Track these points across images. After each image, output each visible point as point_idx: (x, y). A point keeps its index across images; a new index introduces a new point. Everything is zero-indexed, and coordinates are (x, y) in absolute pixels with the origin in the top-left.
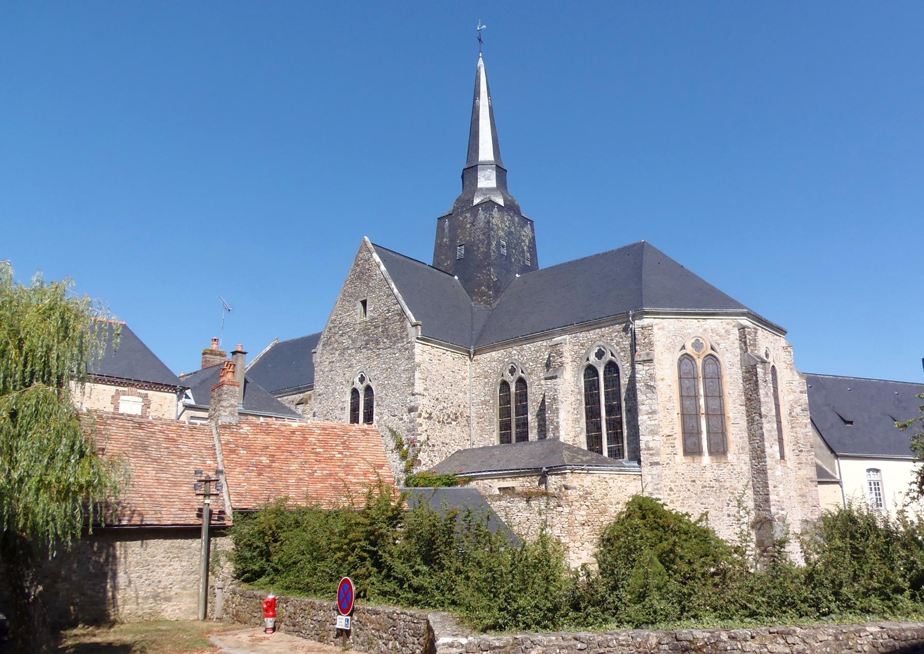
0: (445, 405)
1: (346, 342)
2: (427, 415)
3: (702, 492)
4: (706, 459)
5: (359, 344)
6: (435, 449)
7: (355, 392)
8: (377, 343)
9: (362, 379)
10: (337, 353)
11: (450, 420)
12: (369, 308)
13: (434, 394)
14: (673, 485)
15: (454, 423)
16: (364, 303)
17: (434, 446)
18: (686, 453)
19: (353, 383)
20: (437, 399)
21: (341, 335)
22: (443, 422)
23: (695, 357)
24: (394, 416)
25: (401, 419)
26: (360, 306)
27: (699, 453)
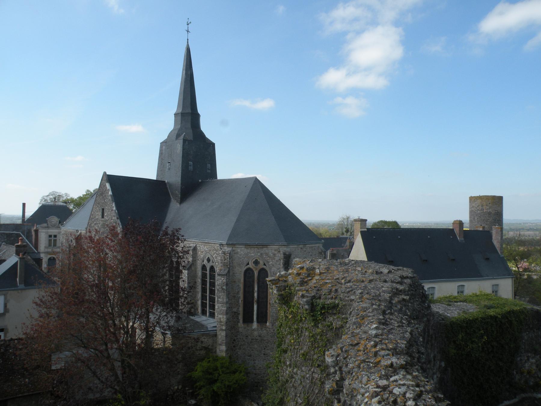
3: (251, 342)
4: (255, 325)
14: (235, 338)
16: (103, 209)
18: (244, 321)
21: (95, 224)
23: (254, 269)
27: (252, 321)
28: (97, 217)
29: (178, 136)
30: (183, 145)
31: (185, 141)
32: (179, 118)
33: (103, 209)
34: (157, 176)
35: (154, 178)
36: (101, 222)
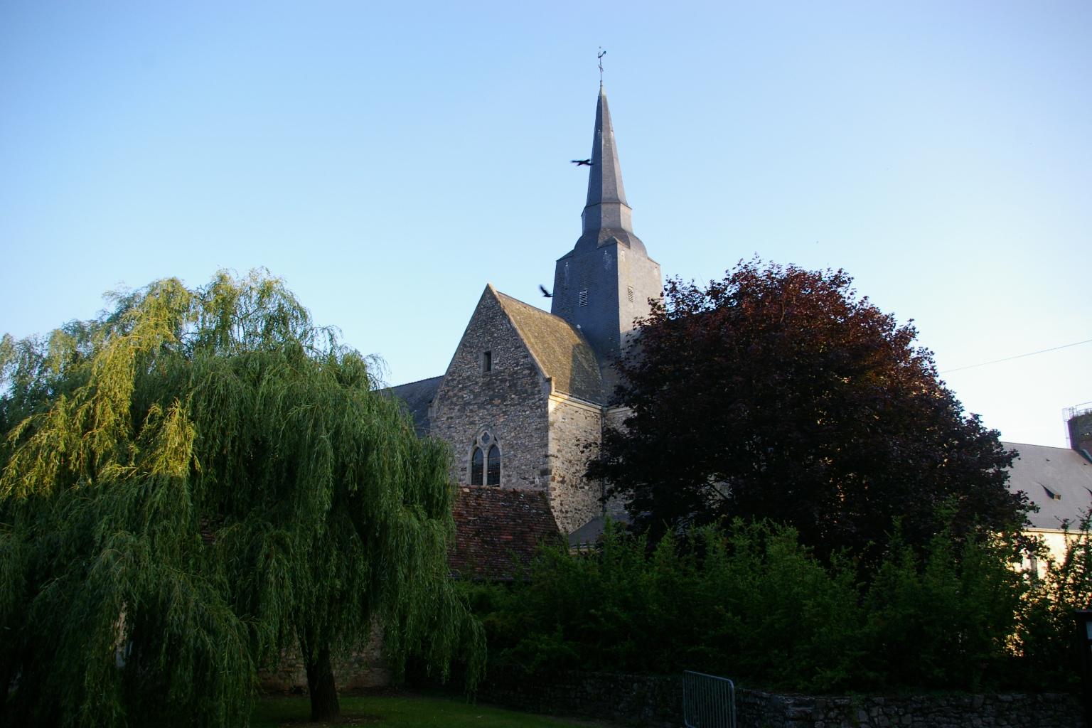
0: (578, 468)
1: (467, 396)
2: (560, 479)
6: (568, 515)
7: (477, 451)
8: (504, 399)
9: (486, 438)
10: (457, 408)
11: (582, 485)
13: (567, 456)
15: (587, 488)
16: (488, 355)
17: (567, 512)
19: (476, 443)
20: (570, 462)
21: (461, 389)
22: (576, 487)
24: (525, 478)
25: (533, 482)
26: (482, 357)
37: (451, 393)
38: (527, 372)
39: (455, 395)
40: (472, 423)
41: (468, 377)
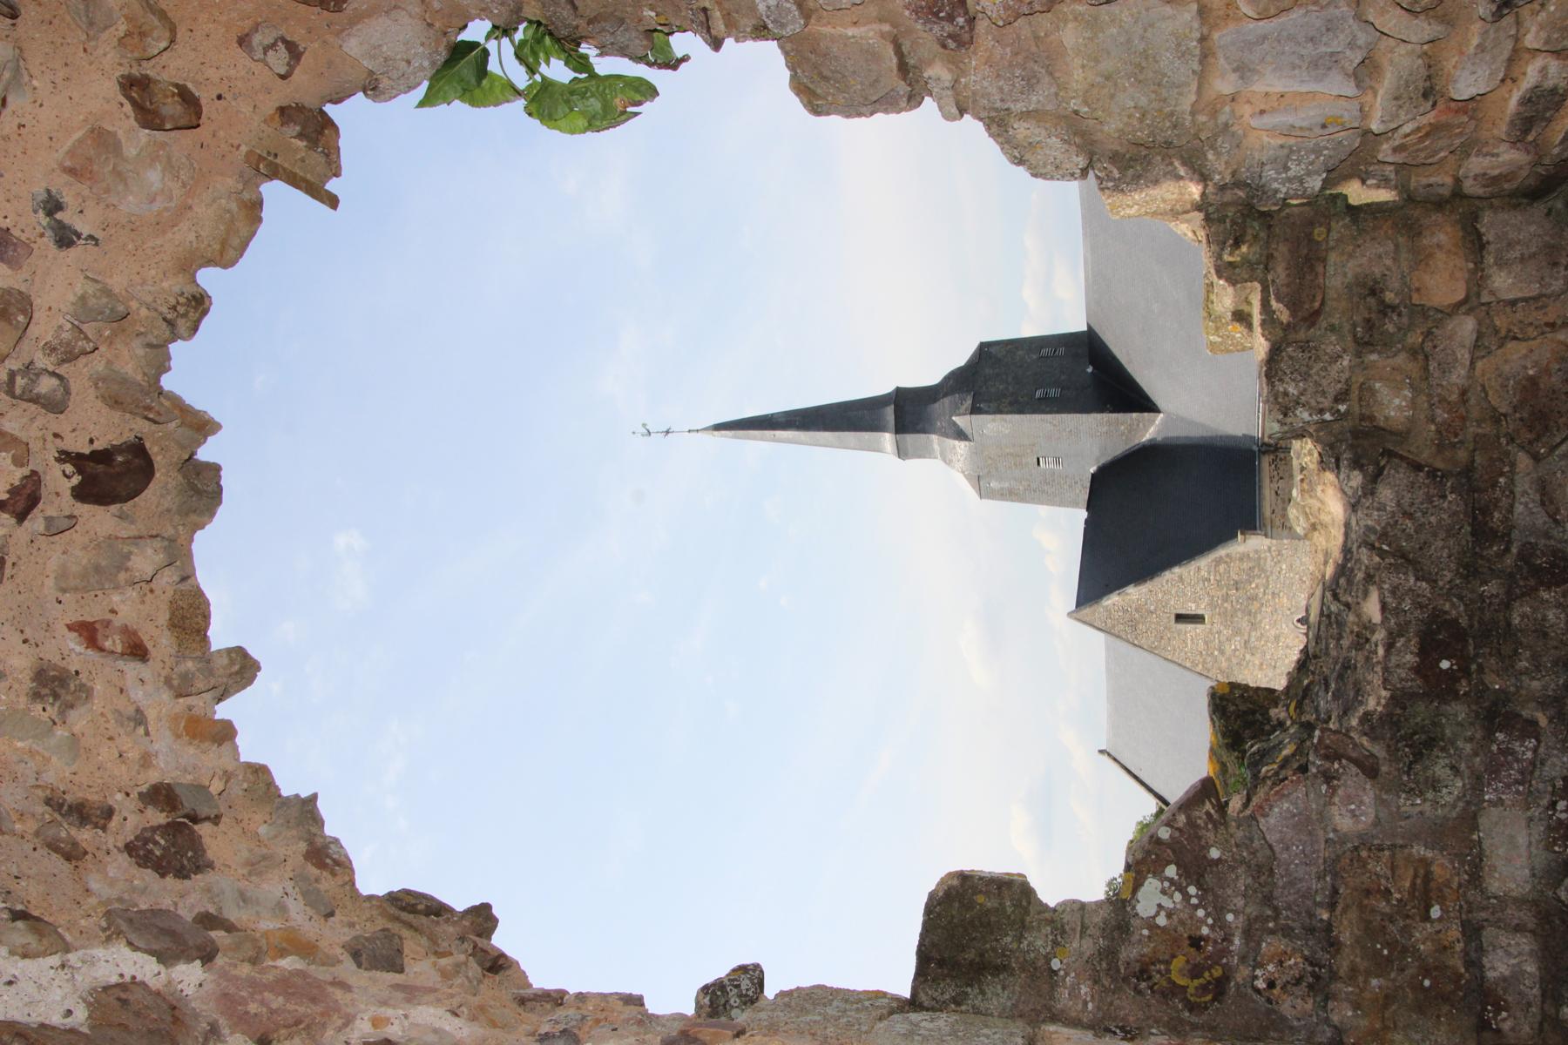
5: (1245, 625)
10: (1248, 657)
12: (1192, 608)
16: (1180, 618)
21: (1222, 652)
28: (1201, 645)
29: (961, 435)
30: (987, 413)
31: (975, 410)
32: (910, 438)
33: (1180, 618)
34: (1075, 505)
35: (1084, 514)
36: (1216, 627)
37: (1224, 665)
38: (1222, 568)
39: (1229, 660)
40: (1277, 638)
41: (1206, 643)
